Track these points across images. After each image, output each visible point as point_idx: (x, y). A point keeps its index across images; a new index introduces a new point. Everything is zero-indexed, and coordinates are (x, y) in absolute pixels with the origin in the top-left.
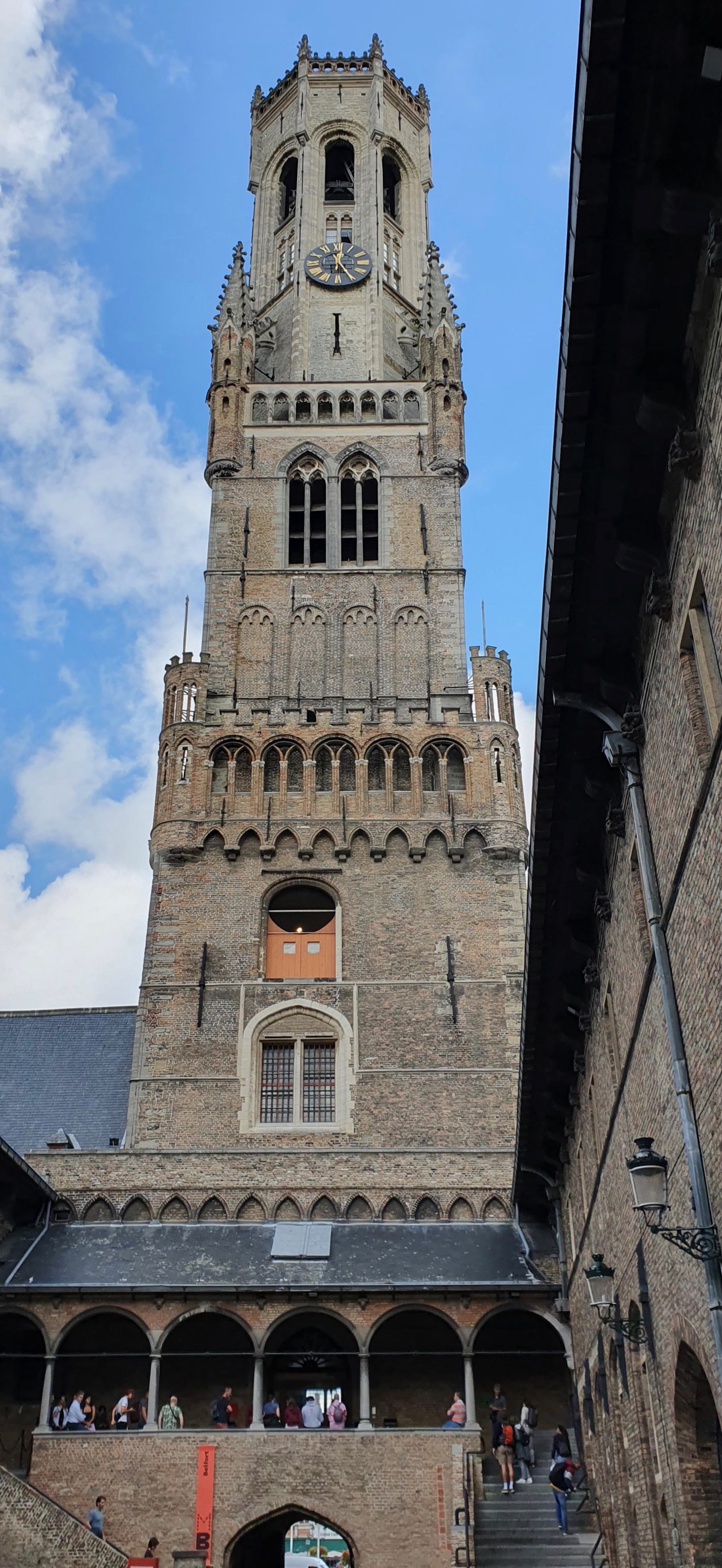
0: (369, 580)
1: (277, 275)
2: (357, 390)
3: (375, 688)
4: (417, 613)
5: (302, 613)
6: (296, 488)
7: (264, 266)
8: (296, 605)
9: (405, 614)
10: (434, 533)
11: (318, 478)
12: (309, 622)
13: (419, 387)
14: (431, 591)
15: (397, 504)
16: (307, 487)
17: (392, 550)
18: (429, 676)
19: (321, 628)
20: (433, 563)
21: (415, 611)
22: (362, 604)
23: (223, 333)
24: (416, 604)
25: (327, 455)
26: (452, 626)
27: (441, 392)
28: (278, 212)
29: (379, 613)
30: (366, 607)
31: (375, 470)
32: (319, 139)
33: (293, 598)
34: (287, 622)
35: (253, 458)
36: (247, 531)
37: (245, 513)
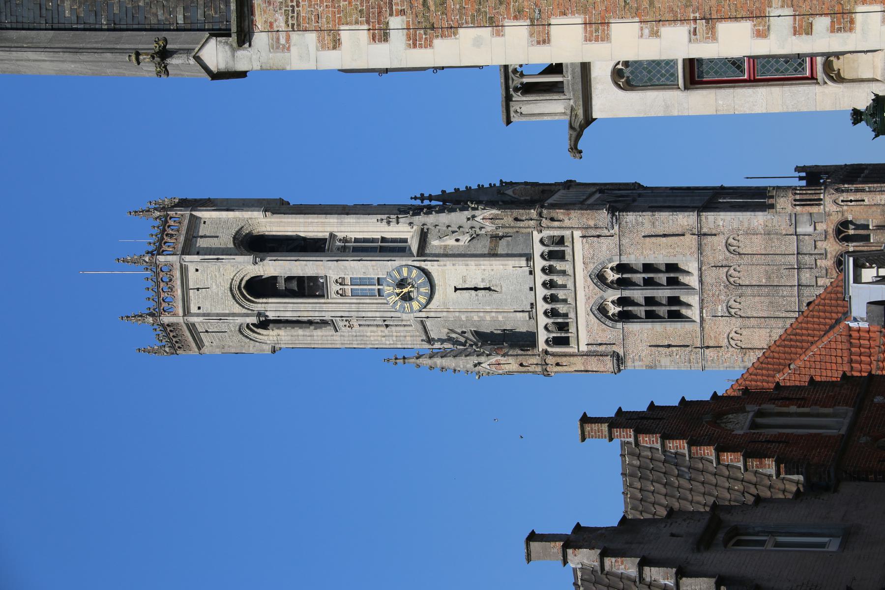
0: (705, 270)
1: (383, 329)
2: (541, 277)
3: (788, 267)
4: (731, 241)
5: (733, 311)
6: (625, 317)
7: (372, 338)
8: (727, 314)
9: (732, 248)
10: (667, 229)
11: (616, 301)
12: (738, 306)
13: (537, 236)
14: (714, 232)
15: (642, 253)
16: (625, 309)
17: (681, 256)
18: (781, 234)
19: (743, 299)
20: (691, 230)
21: (729, 242)
22: (725, 274)
23: (494, 369)
24: (724, 241)
25: (601, 298)
26: (741, 219)
27: (545, 222)
28: (308, 330)
29: (732, 264)
30: (727, 272)
31: (610, 266)
32: (251, 304)
33: (722, 316)
34: (740, 320)
35: (605, 344)
36: (669, 346)
37: (653, 348)
